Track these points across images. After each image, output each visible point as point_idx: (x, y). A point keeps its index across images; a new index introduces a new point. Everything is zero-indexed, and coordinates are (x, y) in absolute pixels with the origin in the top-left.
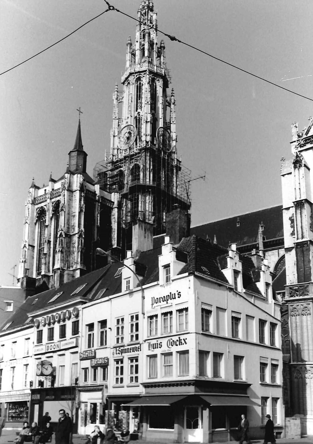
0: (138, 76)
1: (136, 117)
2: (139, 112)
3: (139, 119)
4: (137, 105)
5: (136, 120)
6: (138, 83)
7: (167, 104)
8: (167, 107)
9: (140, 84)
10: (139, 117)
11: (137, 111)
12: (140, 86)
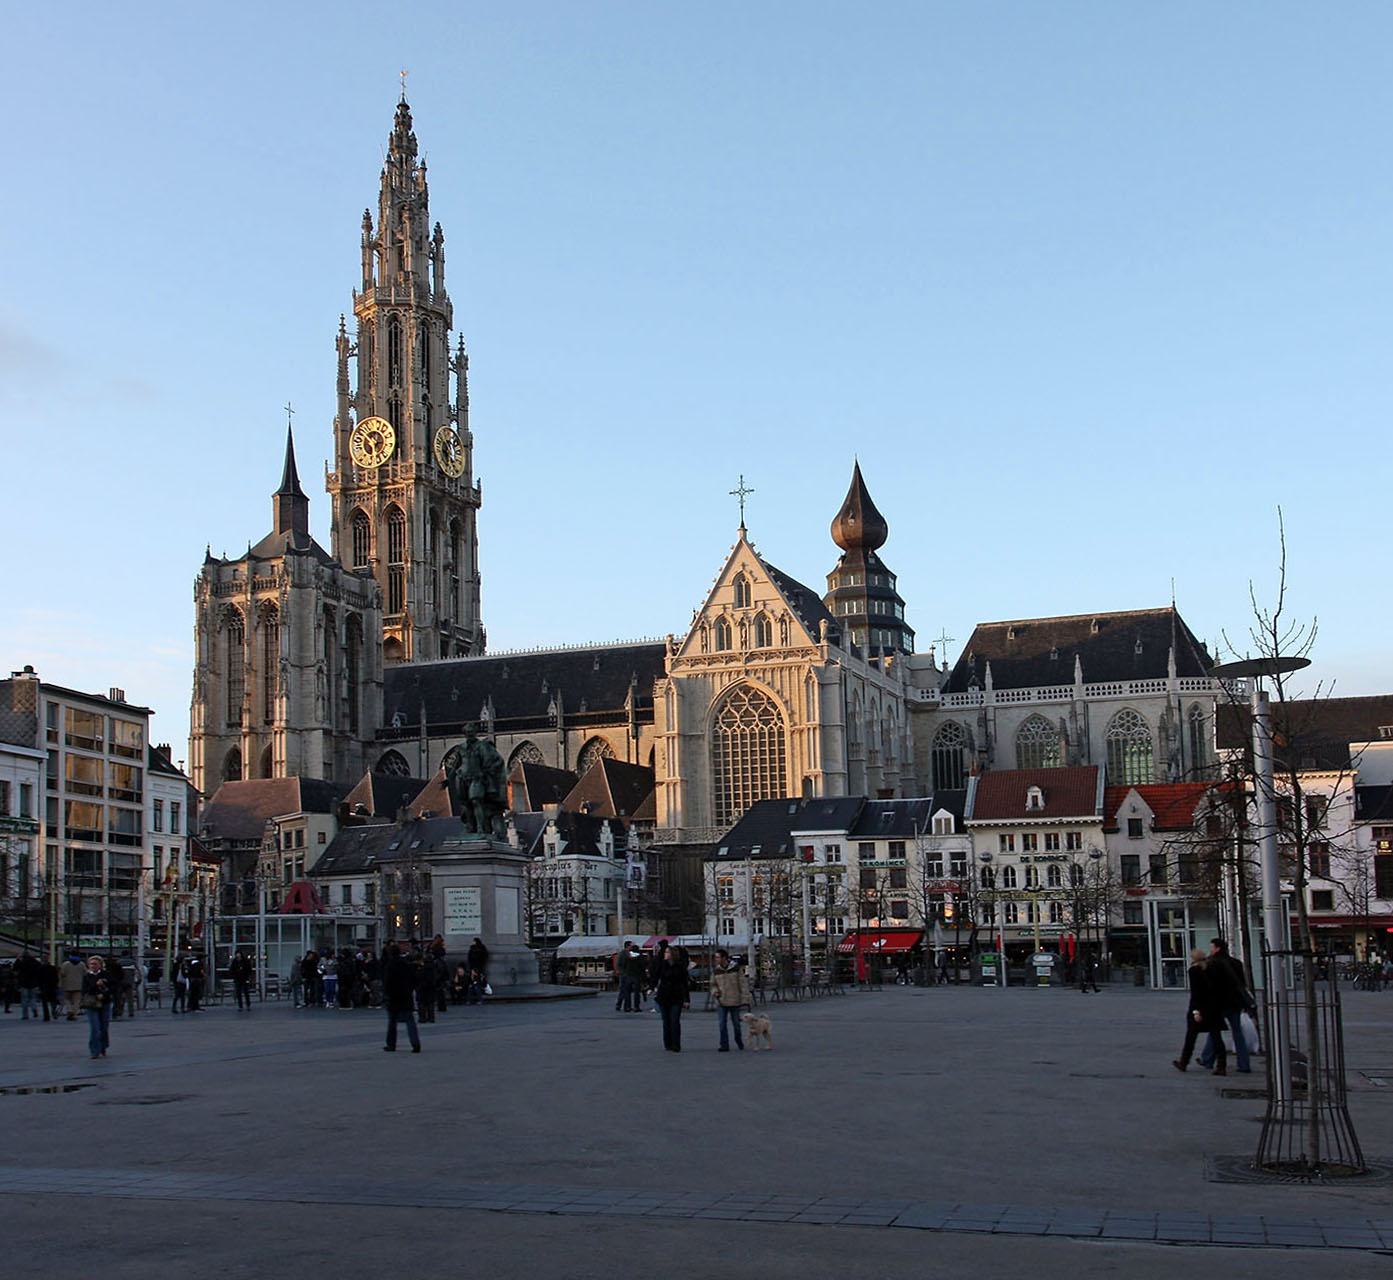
0: (391, 312)
1: (389, 402)
2: (395, 390)
3: (396, 404)
4: (390, 373)
5: (391, 405)
6: (393, 325)
7: (450, 366)
8: (451, 372)
9: (396, 328)
10: (396, 401)
11: (391, 387)
12: (396, 334)
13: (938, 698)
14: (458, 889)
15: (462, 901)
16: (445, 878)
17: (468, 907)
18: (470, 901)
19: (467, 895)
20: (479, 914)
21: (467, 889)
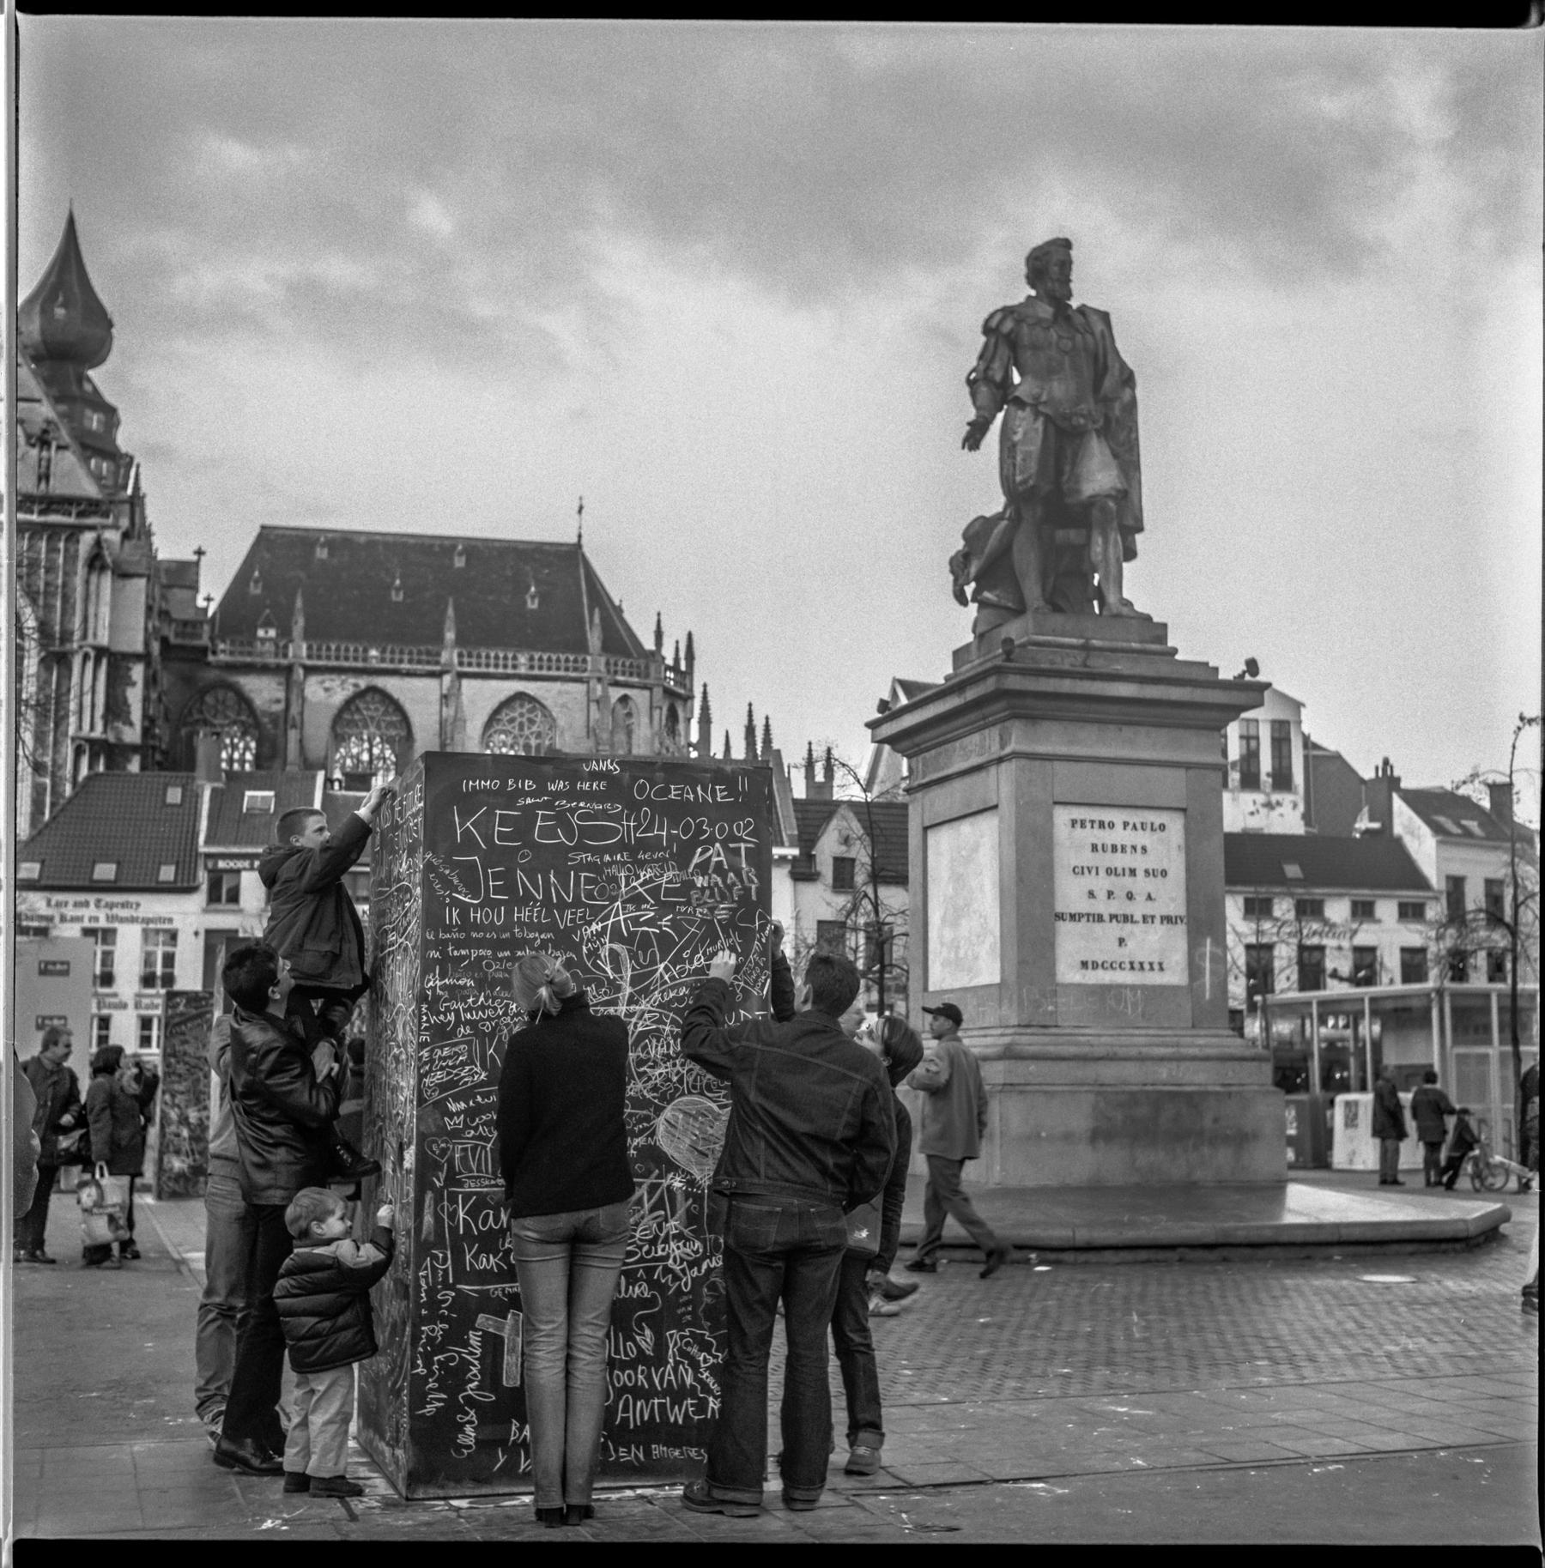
13: (205, 640)
14: (1106, 815)
15: (1120, 861)
16: (1059, 766)
17: (1141, 885)
18: (1150, 862)
19: (1142, 838)
20: (1178, 908)
21: (1135, 817)
